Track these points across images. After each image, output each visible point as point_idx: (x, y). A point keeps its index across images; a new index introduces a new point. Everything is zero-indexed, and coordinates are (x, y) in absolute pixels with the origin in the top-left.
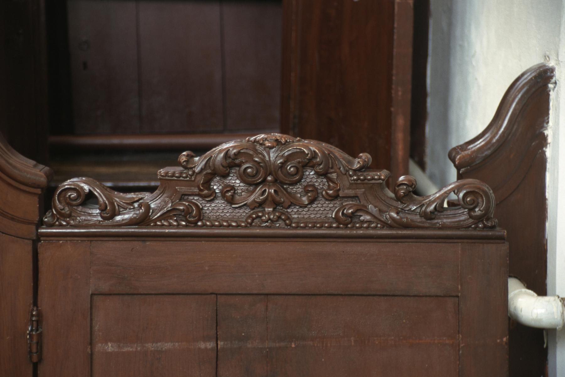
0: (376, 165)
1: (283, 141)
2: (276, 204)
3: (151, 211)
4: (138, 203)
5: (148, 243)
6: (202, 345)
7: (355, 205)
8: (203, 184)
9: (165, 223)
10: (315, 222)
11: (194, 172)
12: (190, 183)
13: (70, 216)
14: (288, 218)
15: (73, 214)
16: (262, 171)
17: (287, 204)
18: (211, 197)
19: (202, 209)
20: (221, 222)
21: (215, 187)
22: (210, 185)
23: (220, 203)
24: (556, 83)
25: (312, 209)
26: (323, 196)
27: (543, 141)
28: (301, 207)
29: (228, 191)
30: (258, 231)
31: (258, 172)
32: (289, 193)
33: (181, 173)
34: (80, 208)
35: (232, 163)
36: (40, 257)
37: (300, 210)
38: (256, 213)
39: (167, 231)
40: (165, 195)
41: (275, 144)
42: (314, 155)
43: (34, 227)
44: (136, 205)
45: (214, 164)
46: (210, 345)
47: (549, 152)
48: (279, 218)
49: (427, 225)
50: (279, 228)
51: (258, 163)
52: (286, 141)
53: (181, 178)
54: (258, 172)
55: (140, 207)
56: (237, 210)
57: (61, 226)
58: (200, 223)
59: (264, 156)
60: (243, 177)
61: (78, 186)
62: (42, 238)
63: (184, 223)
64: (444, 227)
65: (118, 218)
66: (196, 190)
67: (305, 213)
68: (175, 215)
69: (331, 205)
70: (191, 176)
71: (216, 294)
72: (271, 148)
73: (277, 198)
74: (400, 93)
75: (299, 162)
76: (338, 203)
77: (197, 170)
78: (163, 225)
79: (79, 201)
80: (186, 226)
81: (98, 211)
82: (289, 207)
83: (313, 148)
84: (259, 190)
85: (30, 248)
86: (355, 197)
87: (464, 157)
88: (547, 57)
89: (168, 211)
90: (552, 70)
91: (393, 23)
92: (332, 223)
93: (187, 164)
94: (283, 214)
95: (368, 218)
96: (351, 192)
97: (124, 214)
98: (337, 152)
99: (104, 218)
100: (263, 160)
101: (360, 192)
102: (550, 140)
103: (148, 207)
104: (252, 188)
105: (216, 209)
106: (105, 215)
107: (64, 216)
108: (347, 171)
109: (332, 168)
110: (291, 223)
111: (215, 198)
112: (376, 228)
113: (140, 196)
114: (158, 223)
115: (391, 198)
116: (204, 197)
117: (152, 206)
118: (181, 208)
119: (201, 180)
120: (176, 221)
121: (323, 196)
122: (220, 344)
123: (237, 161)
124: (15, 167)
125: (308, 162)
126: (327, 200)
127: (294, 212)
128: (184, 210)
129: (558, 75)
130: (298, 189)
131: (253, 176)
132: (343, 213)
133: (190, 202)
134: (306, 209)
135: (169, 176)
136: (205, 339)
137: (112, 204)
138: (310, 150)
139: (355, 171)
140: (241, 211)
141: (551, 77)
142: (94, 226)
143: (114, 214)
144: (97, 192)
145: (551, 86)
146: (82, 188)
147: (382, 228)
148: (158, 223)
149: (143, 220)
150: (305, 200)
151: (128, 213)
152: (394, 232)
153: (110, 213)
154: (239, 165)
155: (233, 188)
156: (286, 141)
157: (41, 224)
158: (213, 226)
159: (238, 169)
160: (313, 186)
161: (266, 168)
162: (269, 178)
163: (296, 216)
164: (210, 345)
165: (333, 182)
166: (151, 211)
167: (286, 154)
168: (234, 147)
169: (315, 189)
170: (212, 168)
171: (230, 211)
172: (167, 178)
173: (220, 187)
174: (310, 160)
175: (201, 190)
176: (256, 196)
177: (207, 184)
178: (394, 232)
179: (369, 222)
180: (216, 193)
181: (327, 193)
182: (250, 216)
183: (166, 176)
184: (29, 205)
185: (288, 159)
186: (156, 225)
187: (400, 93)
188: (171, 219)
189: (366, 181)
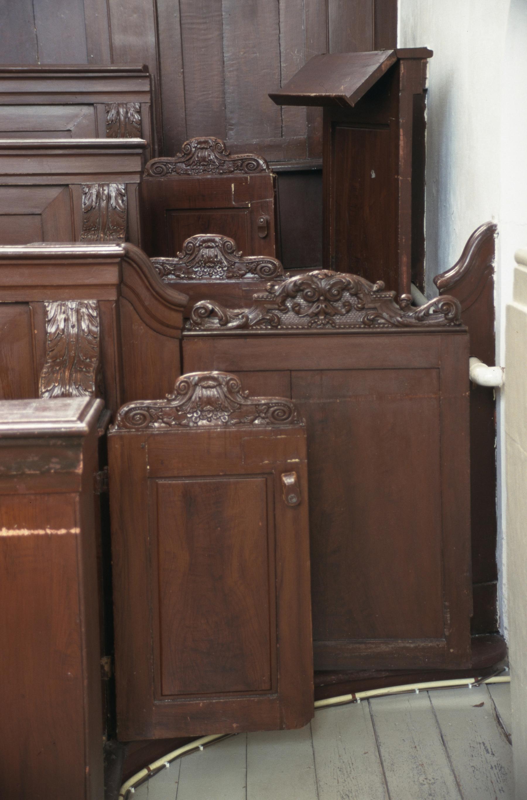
0: (388, 287)
1: (329, 274)
2: (326, 314)
5: (248, 340)
7: (374, 313)
8: (281, 303)
9: (259, 327)
10: (351, 325)
11: (275, 295)
12: (273, 302)
13: (201, 324)
14: (334, 323)
15: (203, 323)
16: (317, 294)
17: (333, 313)
18: (285, 310)
19: (281, 318)
21: (288, 305)
23: (291, 314)
24: (498, 234)
25: (348, 316)
26: (355, 309)
27: (491, 270)
28: (341, 315)
29: (296, 307)
30: (315, 331)
31: (314, 294)
32: (334, 307)
33: (267, 296)
34: (207, 319)
35: (298, 288)
36: (184, 349)
37: (341, 317)
38: (314, 320)
40: (258, 310)
41: (324, 277)
42: (349, 283)
44: (240, 316)
45: (287, 290)
47: (495, 277)
48: (328, 322)
49: (420, 324)
50: (328, 329)
51: (314, 289)
52: (331, 275)
54: (314, 294)
55: (243, 317)
56: (302, 318)
57: (196, 330)
58: (279, 327)
59: (318, 284)
60: (306, 298)
61: (205, 305)
62: (185, 338)
63: (270, 327)
64: (430, 326)
65: (230, 325)
66: (277, 307)
67: (344, 319)
68: (264, 322)
69: (360, 314)
70: (274, 297)
71: (291, 371)
72: (322, 279)
73: (327, 310)
74: (404, 240)
75: (339, 288)
76: (364, 312)
77: (277, 294)
79: (206, 315)
80: (271, 329)
81: (217, 321)
82: (334, 315)
83: (348, 279)
84: (315, 305)
86: (375, 309)
87: (442, 282)
88: (493, 217)
89: (260, 320)
90: (496, 226)
91: (398, 194)
92: (360, 325)
94: (330, 320)
95: (383, 321)
96: (371, 305)
97: (233, 322)
98: (363, 280)
99: (222, 325)
100: (318, 286)
101: (378, 305)
102: (496, 270)
103: (247, 318)
104: (310, 304)
105: (289, 318)
106: (222, 323)
107: (197, 324)
108: (369, 292)
109: (360, 291)
110: (336, 325)
111: (288, 311)
112: (388, 327)
113: (243, 311)
114: (254, 327)
115: (397, 309)
116: (281, 311)
117: (250, 317)
118: (268, 317)
119: (279, 300)
120: (265, 326)
121: (355, 309)
123: (301, 288)
124: (169, 295)
125: (345, 287)
126: (357, 310)
127: (337, 319)
129: (499, 229)
130: (339, 305)
131: (311, 297)
132: (367, 319)
133: (273, 314)
134: (344, 317)
137: (226, 316)
138: (346, 279)
139: (374, 292)
140: (305, 319)
141: (495, 230)
143: (227, 322)
144: (217, 309)
145: (495, 235)
146: (208, 307)
147: (392, 327)
148: (254, 327)
149: (244, 326)
150: (344, 311)
151: (235, 322)
152: (399, 329)
153: (224, 322)
154: (302, 291)
155: (299, 305)
156: (331, 275)
157: (184, 329)
158: (287, 329)
159: (302, 292)
160: (349, 302)
161: (319, 292)
162: (322, 298)
163: (338, 321)
165: (361, 299)
167: (332, 283)
168: (299, 279)
169: (350, 305)
174: (346, 286)
175: (280, 307)
176: (314, 309)
177: (283, 302)
178: (399, 329)
179: (384, 324)
180: (289, 308)
181: (357, 307)
182: (310, 322)
185: (333, 286)
187: (404, 240)
189: (381, 298)
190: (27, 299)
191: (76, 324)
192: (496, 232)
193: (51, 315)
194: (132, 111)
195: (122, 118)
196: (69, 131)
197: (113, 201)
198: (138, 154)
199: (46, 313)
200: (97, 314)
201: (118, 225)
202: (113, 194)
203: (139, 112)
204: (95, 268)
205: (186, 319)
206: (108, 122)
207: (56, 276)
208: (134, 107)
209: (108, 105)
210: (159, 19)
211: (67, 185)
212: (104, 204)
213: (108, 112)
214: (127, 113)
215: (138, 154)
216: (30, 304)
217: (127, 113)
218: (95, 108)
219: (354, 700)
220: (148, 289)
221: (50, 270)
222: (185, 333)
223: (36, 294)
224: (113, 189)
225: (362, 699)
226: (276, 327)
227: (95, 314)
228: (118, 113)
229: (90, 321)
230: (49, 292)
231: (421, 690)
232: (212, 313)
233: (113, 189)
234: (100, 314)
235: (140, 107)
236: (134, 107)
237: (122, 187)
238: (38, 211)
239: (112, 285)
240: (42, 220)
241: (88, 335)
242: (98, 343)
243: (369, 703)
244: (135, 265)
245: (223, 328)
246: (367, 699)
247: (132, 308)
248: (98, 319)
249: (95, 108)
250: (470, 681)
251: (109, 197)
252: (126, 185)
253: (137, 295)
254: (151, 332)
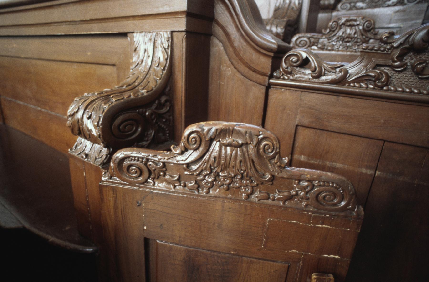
3: (348, 75)
4: (339, 69)
5: (341, 98)
6: (364, 171)
13: (291, 73)
15: (293, 72)
20: (405, 88)
22: (403, 59)
33: (380, 47)
34: (298, 69)
39: (357, 90)
40: (362, 64)
43: (267, 78)
44: (338, 70)
46: (369, 172)
53: (379, 52)
57: (284, 79)
61: (299, 53)
62: (272, 86)
63: (372, 86)
65: (323, 78)
66: (390, 62)
68: (366, 80)
70: (389, 49)
71: (385, 141)
77: (395, 45)
78: (355, 86)
81: (310, 72)
85: (264, 91)
93: (387, 39)
97: (328, 75)
99: (314, 77)
103: (346, 72)
106: (315, 75)
107: (287, 73)
114: (352, 85)
117: (350, 71)
118: (373, 74)
119: (397, 53)
120: (366, 84)
122: (378, 173)
128: (374, 77)
135: (369, 50)
136: (367, 167)
142: (305, 81)
143: (320, 75)
146: (301, 55)
149: (341, 81)
151: (331, 75)
157: (271, 77)
164: (369, 172)
166: (348, 75)
170: (410, 43)
171: (417, 80)
172: (367, 50)
173: (413, 61)
180: (407, 65)
183: (366, 49)
184: (265, 63)
186: (349, 86)
188: (362, 83)
190: (125, 31)
205: (275, 66)
216: (128, 35)
222: (271, 81)
226: (381, 88)
230: (137, 22)
232: (305, 63)
245: (314, 80)
247: (222, 48)
253: (227, 34)
254: (238, 75)
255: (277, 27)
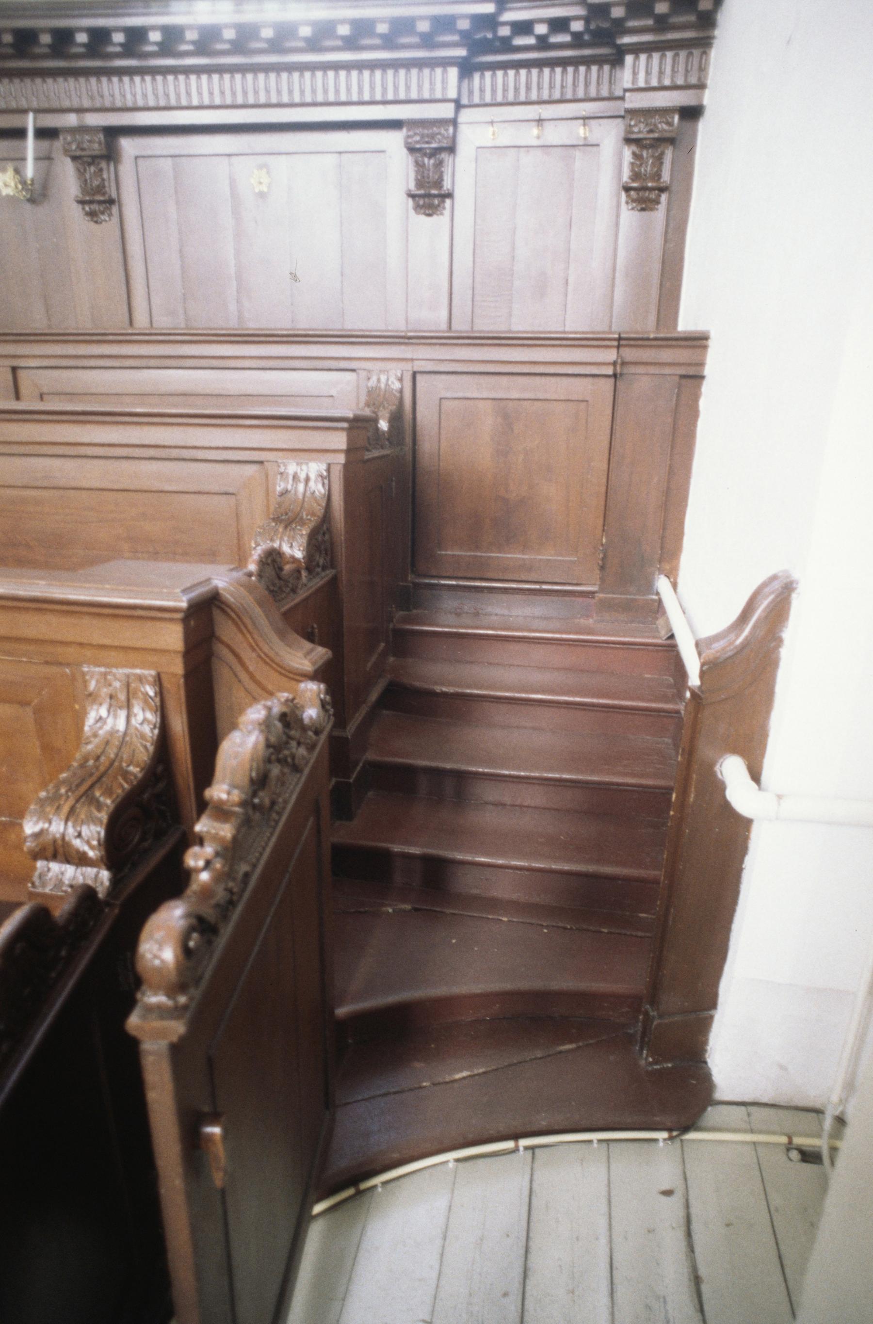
141: (796, 589)
191: (125, 704)
192: (796, 591)
193: (92, 685)
194: (392, 379)
195: (383, 386)
196: (332, 396)
197: (312, 484)
198: (342, 429)
199: (85, 683)
200: (156, 693)
201: (313, 514)
202: (313, 476)
203: (401, 380)
204: (150, 624)
206: (367, 388)
207: (97, 631)
208: (396, 375)
209: (369, 371)
210: (453, 296)
211: (261, 462)
212: (301, 487)
213: (369, 379)
214: (388, 380)
215: (342, 429)
217: (388, 380)
218: (358, 374)
219: (516, 1150)
220: (254, 650)
221: (86, 621)
223: (71, 652)
224: (315, 468)
225: (526, 1148)
227: (151, 693)
228: (379, 380)
229: (146, 702)
231: (600, 1141)
233: (315, 468)
234: (161, 693)
235: (402, 375)
236: (396, 375)
237: (323, 467)
238: (231, 490)
239: (175, 652)
240: (237, 500)
241: (142, 724)
242: (155, 738)
243: (533, 1154)
244: (233, 614)
246: (532, 1148)
248: (158, 700)
249: (358, 374)
250: (665, 1135)
251: (307, 480)
252: (329, 466)
255: (291, 547)
